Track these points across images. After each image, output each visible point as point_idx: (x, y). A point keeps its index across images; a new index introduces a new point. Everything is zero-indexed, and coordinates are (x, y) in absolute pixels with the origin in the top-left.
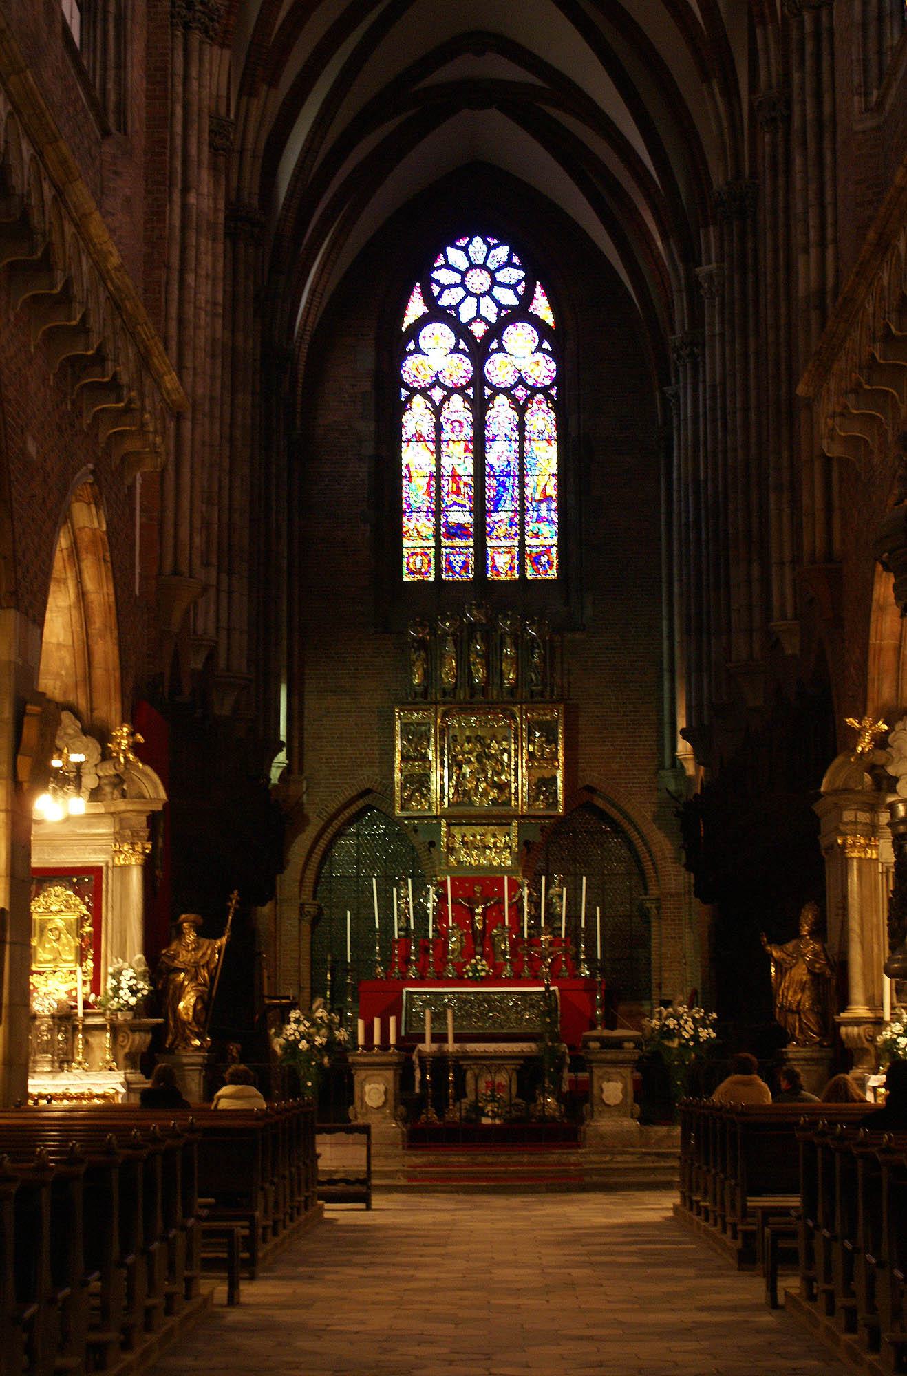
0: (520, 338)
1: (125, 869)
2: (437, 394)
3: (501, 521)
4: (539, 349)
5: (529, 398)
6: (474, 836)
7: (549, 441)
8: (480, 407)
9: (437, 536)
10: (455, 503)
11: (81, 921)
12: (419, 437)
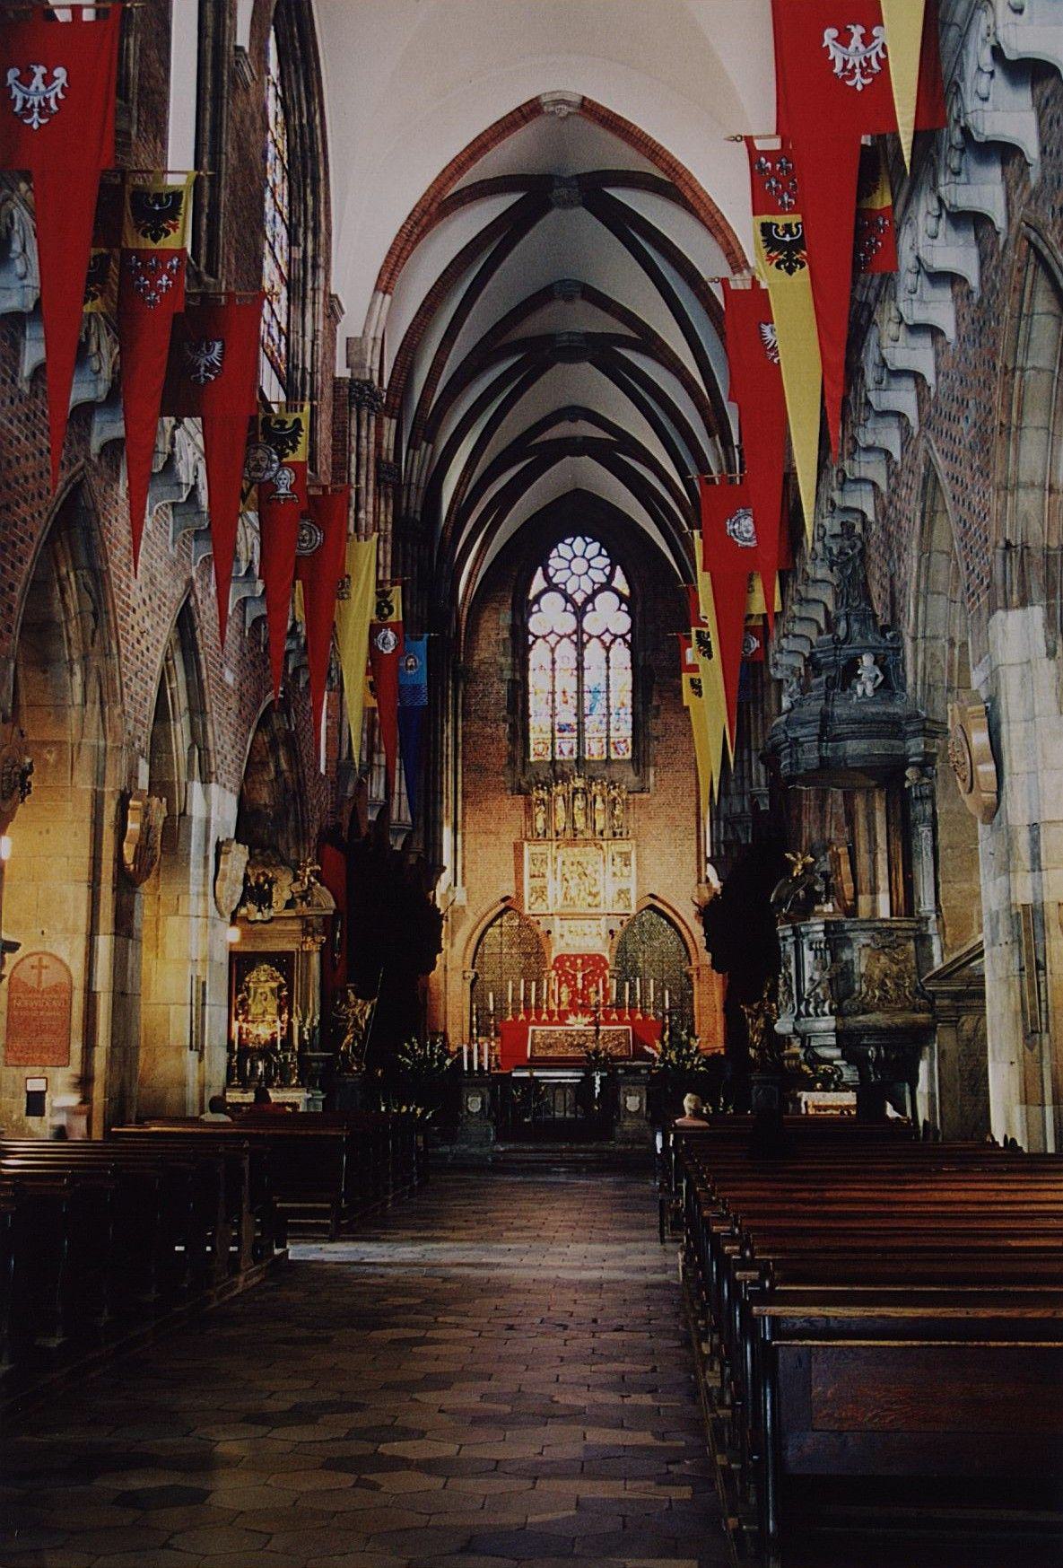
0: (607, 601)
1: (308, 954)
2: (552, 639)
5: (612, 642)
8: (580, 646)
9: (553, 731)
11: (280, 988)
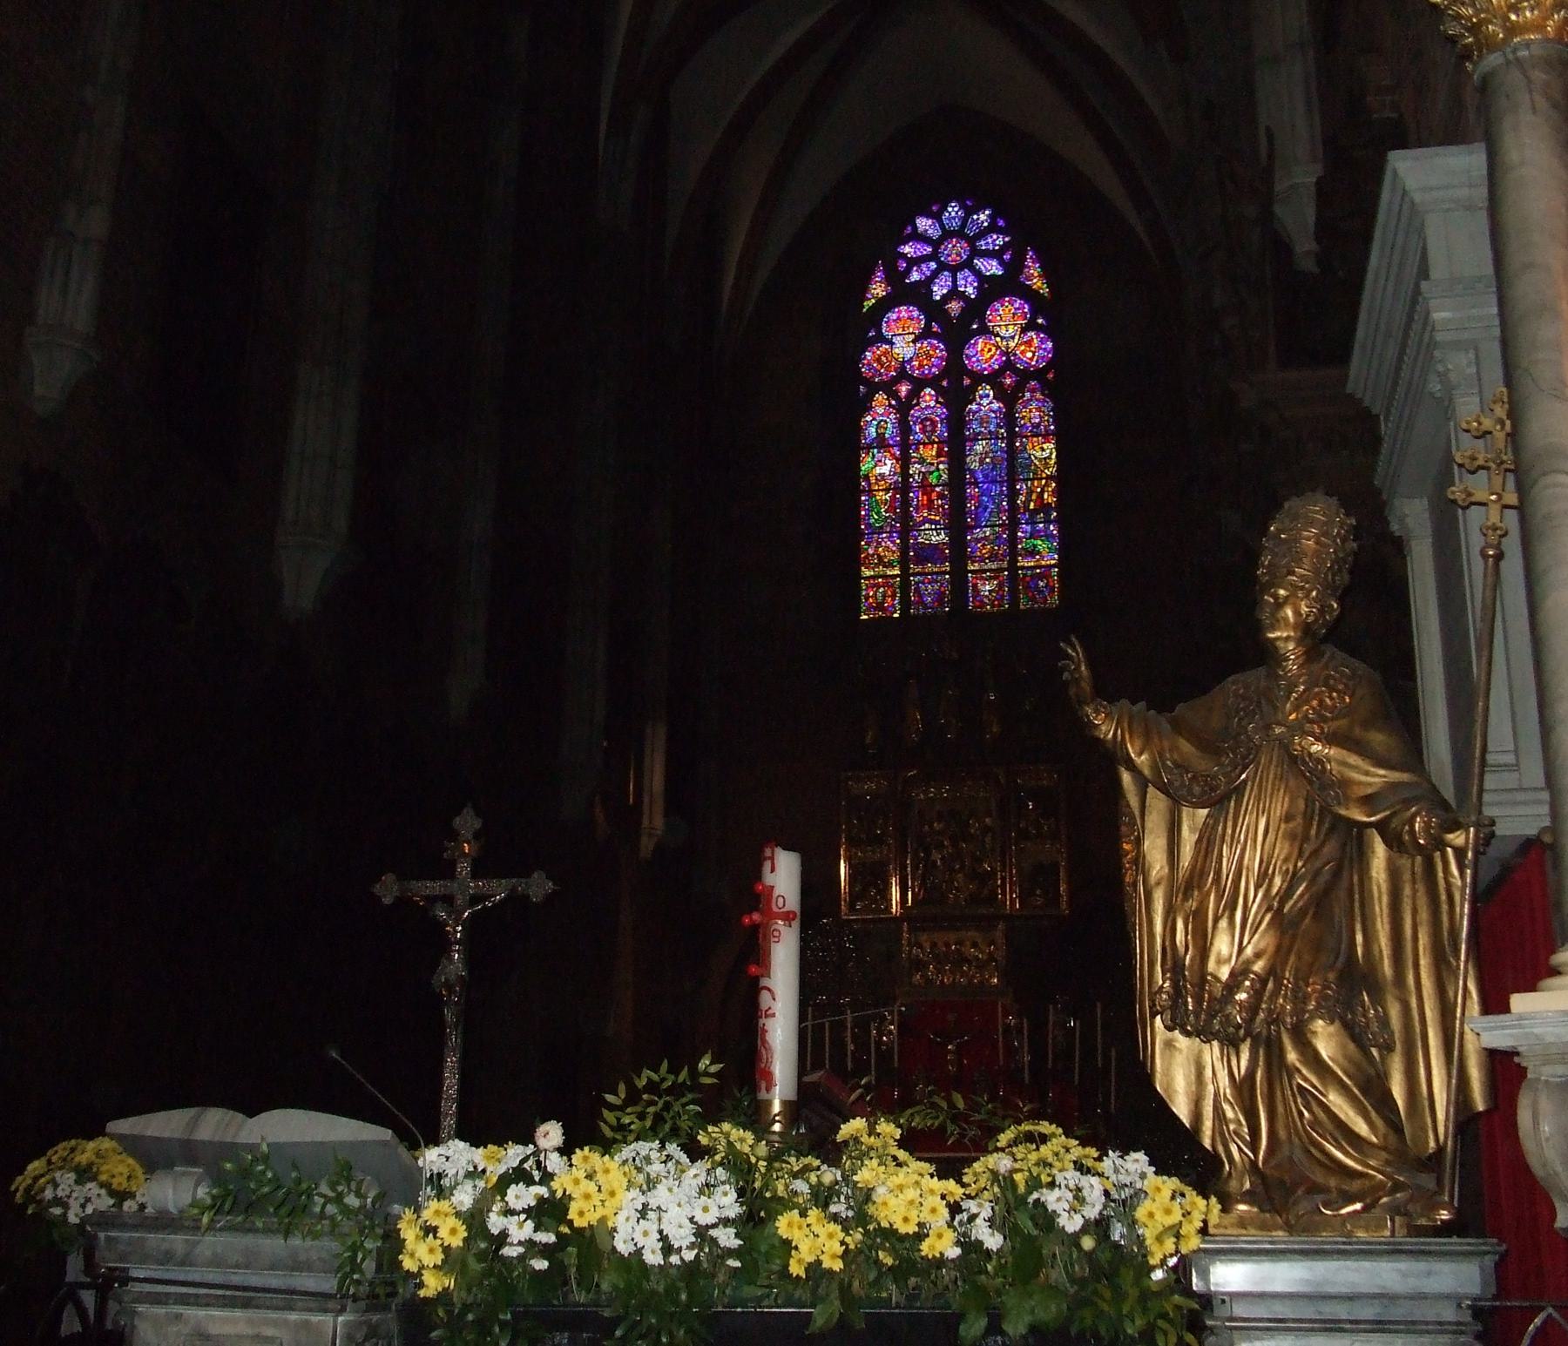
3: (986, 538)
4: (1030, 326)
5: (1019, 387)
6: (948, 945)
7: (1046, 436)
9: (904, 562)
10: (926, 520)
12: (881, 443)
